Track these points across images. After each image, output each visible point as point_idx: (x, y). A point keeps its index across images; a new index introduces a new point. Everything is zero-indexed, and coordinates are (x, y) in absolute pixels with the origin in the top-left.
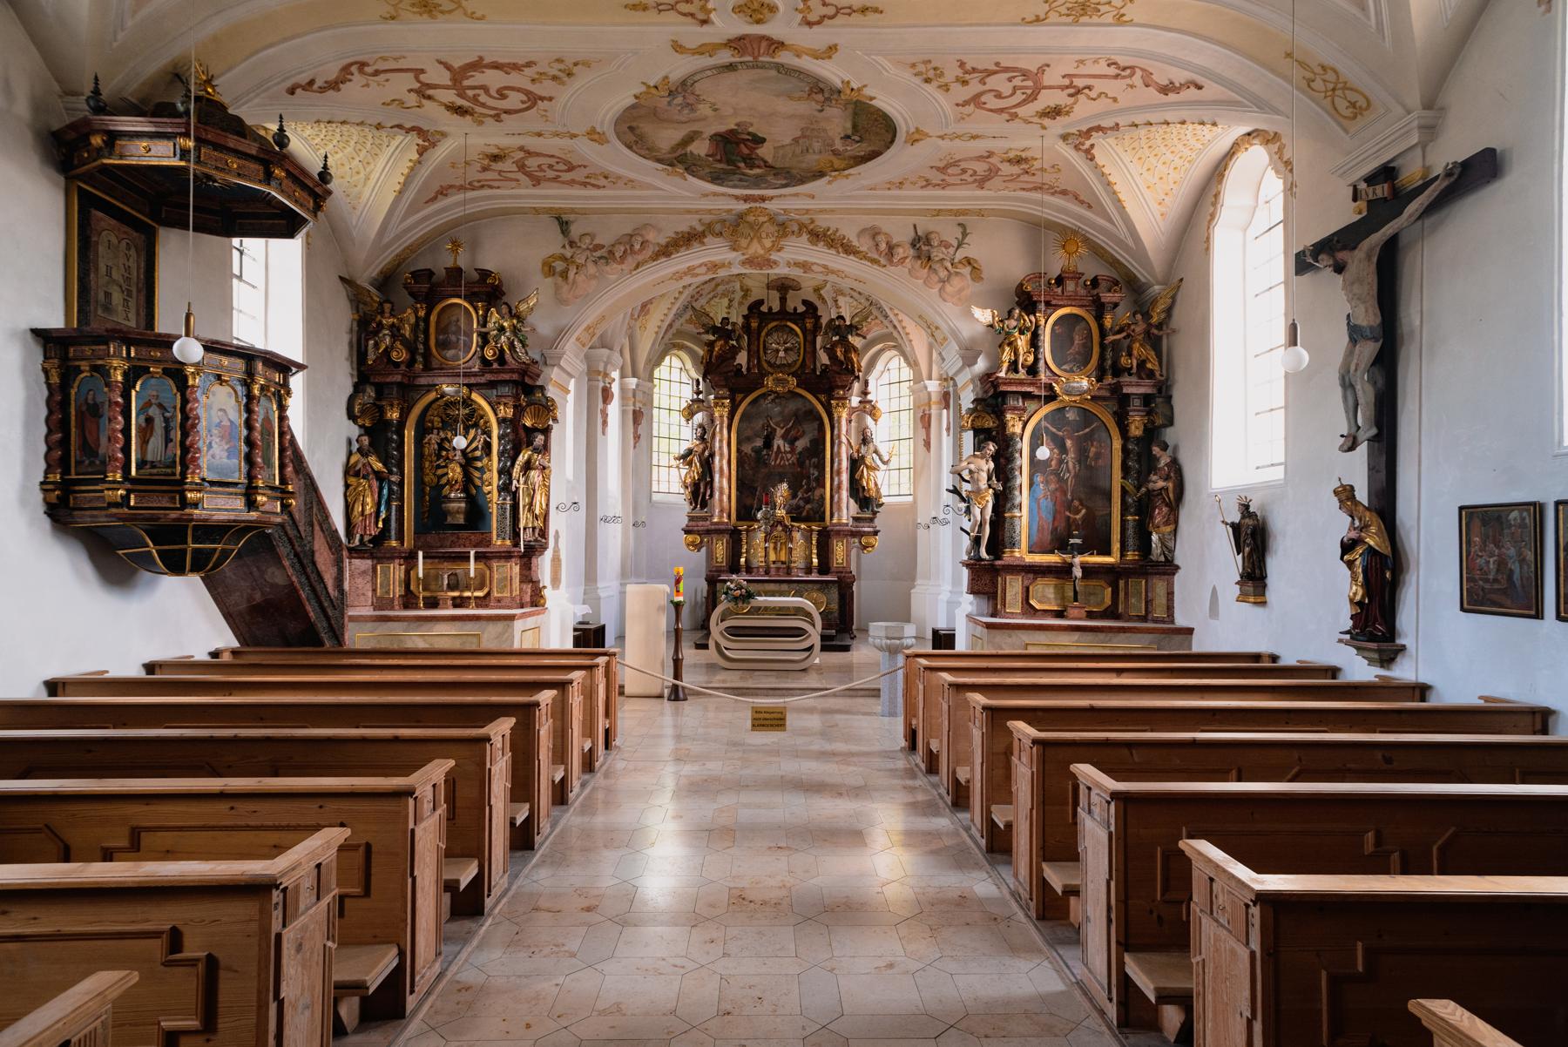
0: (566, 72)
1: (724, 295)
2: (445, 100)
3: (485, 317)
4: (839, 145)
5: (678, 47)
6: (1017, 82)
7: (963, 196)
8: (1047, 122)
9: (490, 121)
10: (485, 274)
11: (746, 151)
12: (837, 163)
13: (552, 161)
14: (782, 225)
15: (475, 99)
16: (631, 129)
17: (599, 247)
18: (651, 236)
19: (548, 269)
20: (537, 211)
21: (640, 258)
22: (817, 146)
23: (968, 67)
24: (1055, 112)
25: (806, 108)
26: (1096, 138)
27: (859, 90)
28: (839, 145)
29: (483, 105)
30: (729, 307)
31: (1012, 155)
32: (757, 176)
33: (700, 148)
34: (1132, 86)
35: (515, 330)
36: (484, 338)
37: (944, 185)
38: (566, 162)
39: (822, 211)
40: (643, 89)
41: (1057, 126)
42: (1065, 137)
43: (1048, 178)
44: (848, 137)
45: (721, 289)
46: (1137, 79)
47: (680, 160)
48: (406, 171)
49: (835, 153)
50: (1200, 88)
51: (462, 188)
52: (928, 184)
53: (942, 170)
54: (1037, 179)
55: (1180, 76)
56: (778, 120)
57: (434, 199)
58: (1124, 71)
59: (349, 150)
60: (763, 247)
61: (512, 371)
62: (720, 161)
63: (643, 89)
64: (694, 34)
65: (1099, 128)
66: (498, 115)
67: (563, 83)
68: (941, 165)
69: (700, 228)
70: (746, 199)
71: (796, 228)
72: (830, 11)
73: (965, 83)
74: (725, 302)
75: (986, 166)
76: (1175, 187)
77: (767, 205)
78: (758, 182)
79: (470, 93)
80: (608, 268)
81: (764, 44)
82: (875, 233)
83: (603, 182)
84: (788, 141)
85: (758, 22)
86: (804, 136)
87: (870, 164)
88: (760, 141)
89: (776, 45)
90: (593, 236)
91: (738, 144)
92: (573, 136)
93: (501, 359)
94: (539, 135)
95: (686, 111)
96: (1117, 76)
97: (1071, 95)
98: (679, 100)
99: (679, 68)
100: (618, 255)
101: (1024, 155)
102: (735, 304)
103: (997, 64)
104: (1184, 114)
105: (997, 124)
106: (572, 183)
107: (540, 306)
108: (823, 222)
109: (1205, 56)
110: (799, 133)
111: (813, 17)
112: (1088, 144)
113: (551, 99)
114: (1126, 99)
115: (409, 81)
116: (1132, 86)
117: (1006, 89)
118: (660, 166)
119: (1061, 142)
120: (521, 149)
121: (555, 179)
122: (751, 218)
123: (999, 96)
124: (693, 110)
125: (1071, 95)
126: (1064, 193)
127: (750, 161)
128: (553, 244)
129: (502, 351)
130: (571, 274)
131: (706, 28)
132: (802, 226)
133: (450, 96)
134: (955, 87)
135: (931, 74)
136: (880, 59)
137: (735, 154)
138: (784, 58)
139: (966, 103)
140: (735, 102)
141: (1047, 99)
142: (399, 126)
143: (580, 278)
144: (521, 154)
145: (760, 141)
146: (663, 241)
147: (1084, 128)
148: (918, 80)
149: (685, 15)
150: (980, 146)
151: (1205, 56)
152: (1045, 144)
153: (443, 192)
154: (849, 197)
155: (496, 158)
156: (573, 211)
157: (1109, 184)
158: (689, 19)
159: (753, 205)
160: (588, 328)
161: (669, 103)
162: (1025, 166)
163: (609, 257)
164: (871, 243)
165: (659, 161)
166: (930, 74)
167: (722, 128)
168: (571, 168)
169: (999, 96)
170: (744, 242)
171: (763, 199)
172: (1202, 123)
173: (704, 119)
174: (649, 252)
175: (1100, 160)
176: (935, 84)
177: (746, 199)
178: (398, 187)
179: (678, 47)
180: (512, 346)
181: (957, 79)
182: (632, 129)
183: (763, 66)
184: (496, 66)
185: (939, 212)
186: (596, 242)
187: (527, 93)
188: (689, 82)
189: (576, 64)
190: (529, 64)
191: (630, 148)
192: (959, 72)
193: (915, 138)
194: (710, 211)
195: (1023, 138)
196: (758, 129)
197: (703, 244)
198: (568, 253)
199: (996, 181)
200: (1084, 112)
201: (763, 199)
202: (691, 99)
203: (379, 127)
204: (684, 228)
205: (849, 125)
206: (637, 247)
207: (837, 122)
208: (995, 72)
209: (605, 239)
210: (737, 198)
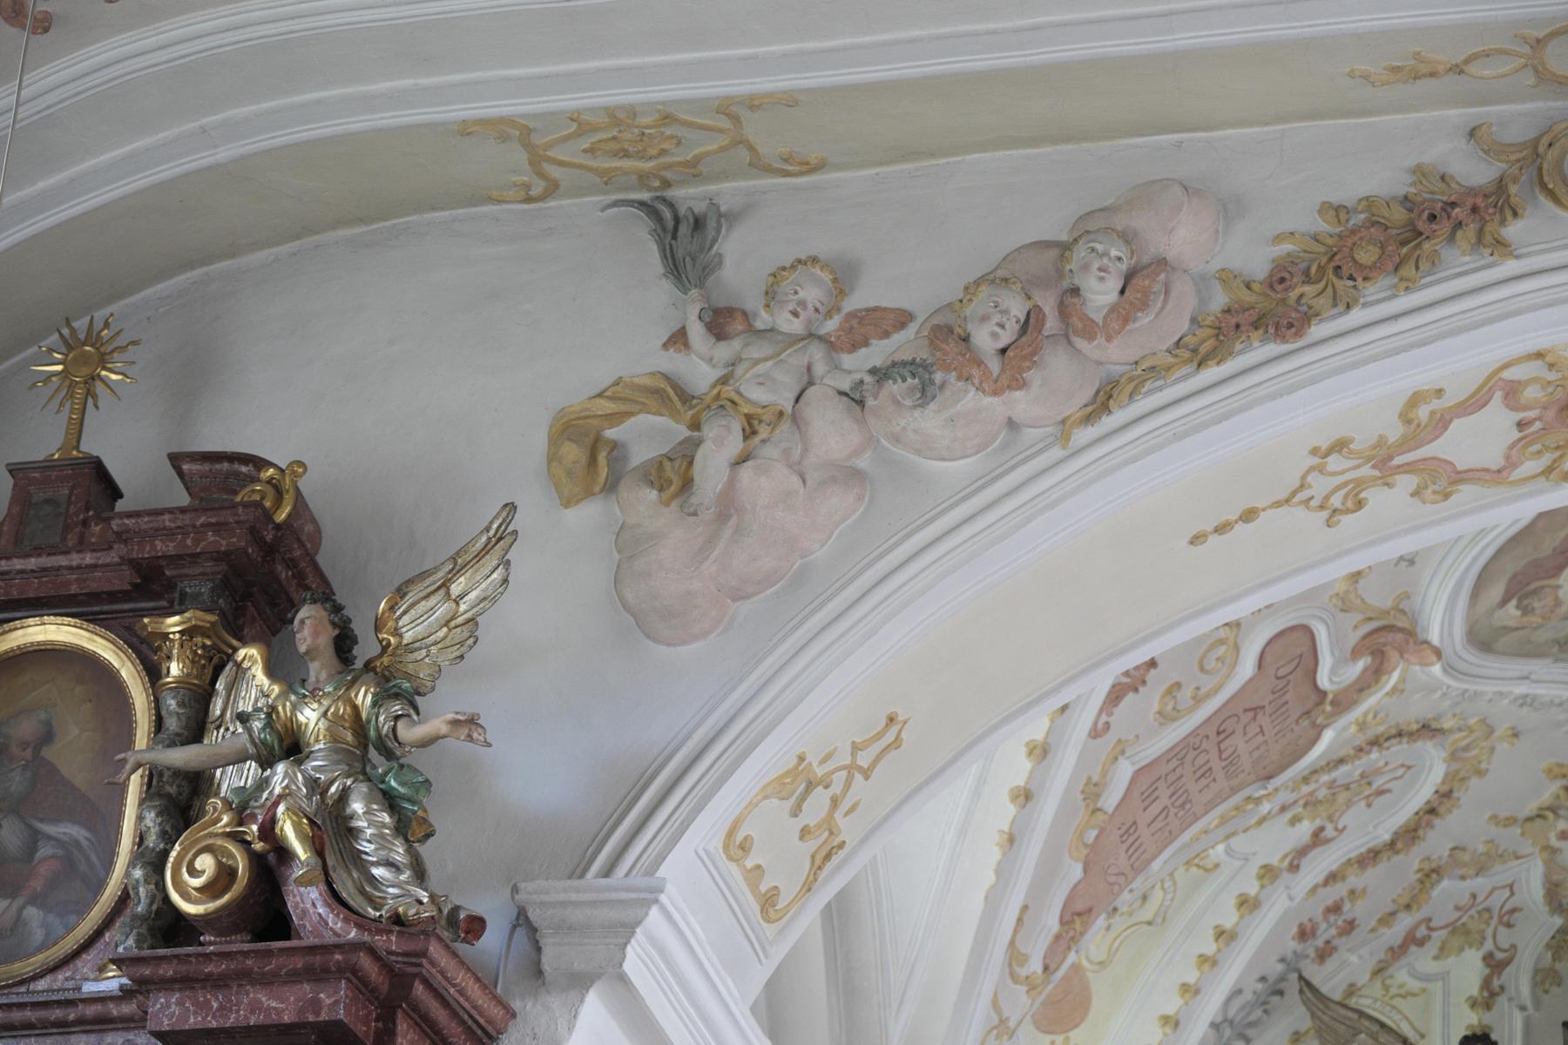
1: (1462, 933)
3: (199, 697)
10: (220, 476)
18: (1184, 238)
19: (588, 455)
21: (1116, 354)
30: (1489, 996)
35: (363, 747)
36: (182, 799)
45: (1449, 893)
61: (322, 964)
69: (1475, 172)
74: (1468, 970)
80: (929, 421)
90: (843, 277)
93: (262, 910)
100: (986, 339)
102: (1520, 979)
107: (526, 680)
128: (612, 325)
129: (270, 864)
130: (713, 462)
143: (763, 484)
146: (1253, 256)
160: (799, 783)
163: (938, 355)
174: (1167, 321)
180: (330, 829)
186: (858, 300)
197: (1502, 247)
198: (699, 368)
204: (1375, 173)
206: (1101, 294)
209: (911, 277)
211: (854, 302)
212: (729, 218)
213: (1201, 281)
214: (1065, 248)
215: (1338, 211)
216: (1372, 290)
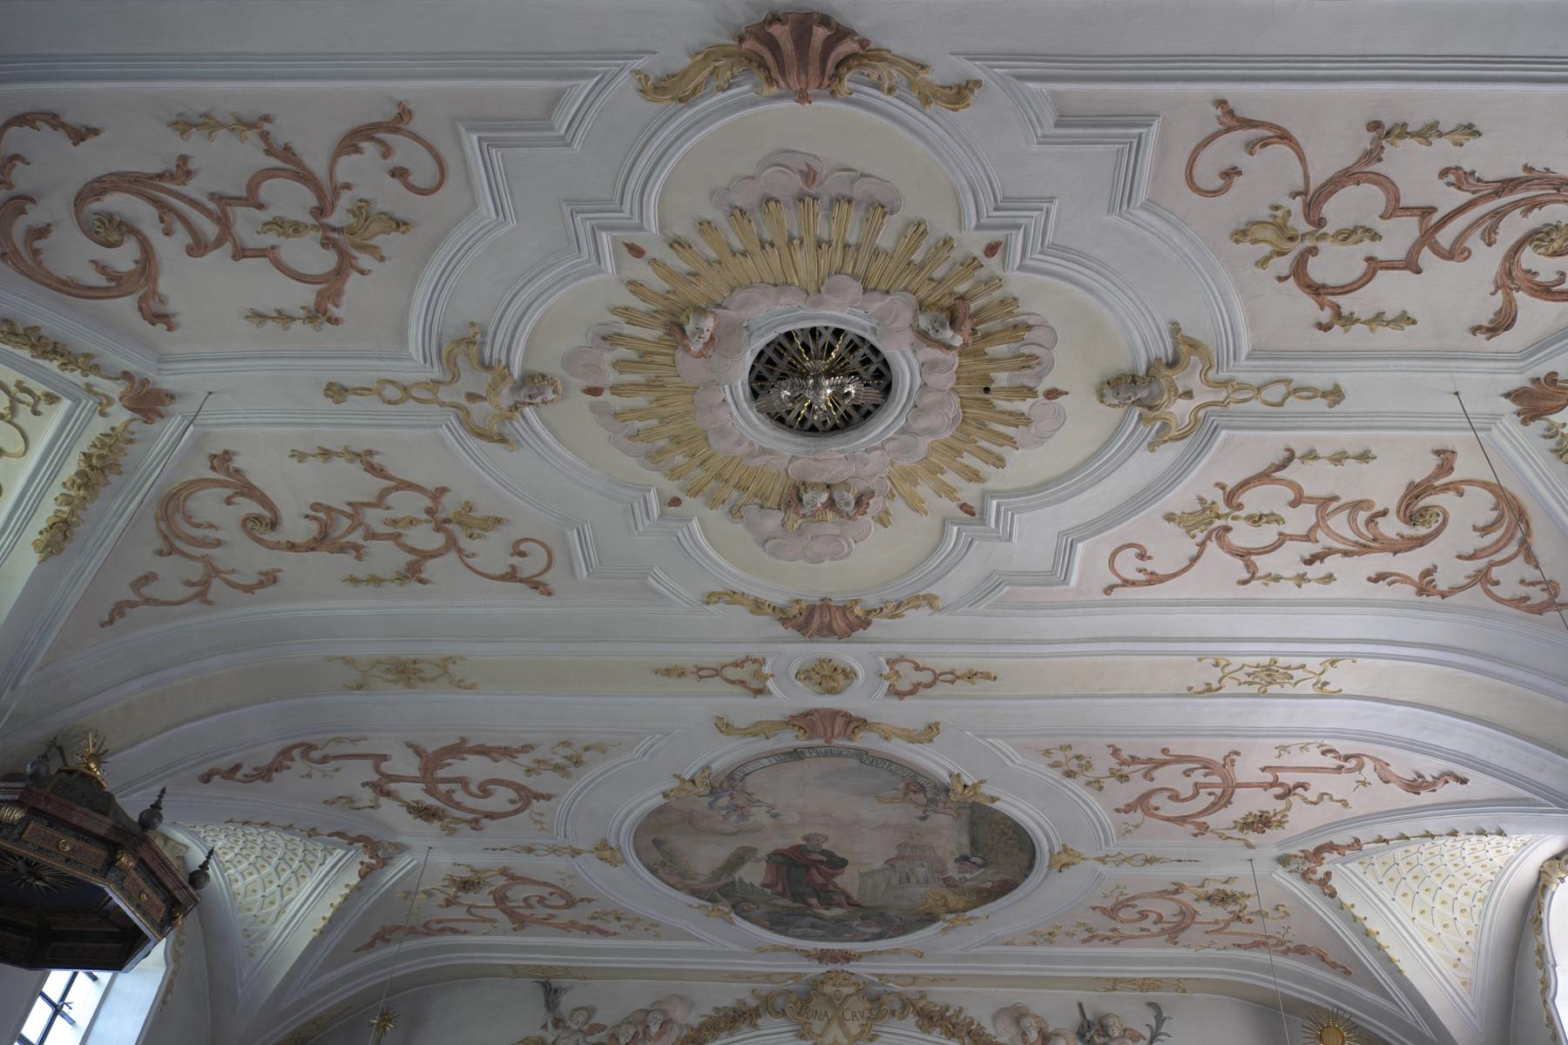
0: (573, 761)
2: (408, 799)
4: (953, 871)
5: (724, 726)
6: (1198, 776)
7: (1148, 957)
8: (1252, 837)
9: (465, 828)
11: (819, 879)
12: (953, 900)
13: (544, 891)
14: (876, 1000)
15: (448, 798)
16: (657, 843)
17: (598, 1028)
18: (679, 1014)
20: (515, 972)
22: (921, 872)
23: (1125, 755)
24: (1261, 822)
25: (901, 814)
26: (1330, 862)
27: (974, 786)
28: (953, 871)
29: (458, 805)
31: (1210, 889)
32: (838, 920)
33: (754, 874)
34: (1364, 783)
37: (1116, 939)
38: (563, 894)
39: (937, 980)
40: (676, 783)
41: (1269, 843)
42: (1284, 861)
43: (1273, 927)
44: (965, 858)
46: (1369, 772)
47: (724, 893)
48: (337, 901)
49: (949, 883)
50: (1464, 781)
51: (413, 932)
52: (1091, 937)
53: (1111, 912)
54: (1257, 928)
55: (1431, 767)
56: (865, 832)
57: (369, 946)
58: (1348, 763)
59: (268, 869)
60: (847, 1034)
62: (782, 894)
63: (676, 783)
64: (745, 709)
65: (1331, 847)
66: (476, 821)
67: (567, 775)
68: (1108, 904)
69: (752, 1003)
70: (822, 957)
71: (897, 1006)
72: (926, 677)
73: (1123, 778)
75: (1175, 908)
76: (1468, 938)
77: (851, 967)
78: (838, 930)
79: (443, 788)
81: (840, 722)
82: (1018, 1015)
83: (613, 926)
84: (879, 864)
85: (831, 691)
86: (901, 857)
87: (1002, 901)
88: (838, 864)
89: (854, 724)
90: (591, 1011)
91: (807, 868)
92: (576, 853)
94: (530, 850)
95: (734, 818)
96: (1339, 769)
97: (1278, 797)
98: (724, 801)
99: (725, 753)
101: (1229, 889)
103: (1165, 751)
104: (1452, 821)
105: (1178, 841)
106: (571, 927)
108: (940, 995)
109: (1461, 737)
110: (894, 853)
111: (903, 686)
112: (1320, 872)
113: (548, 797)
114: (1361, 803)
115: (366, 771)
116: (1364, 783)
117: (1185, 787)
118: (695, 901)
119: (1280, 870)
120: (504, 872)
121: (545, 921)
122: (829, 989)
123: (1175, 797)
124: (743, 816)
125: (1278, 797)
126: (1301, 950)
127: (827, 896)
131: (760, 700)
132: (907, 1004)
133: (414, 793)
134: (1111, 784)
135: (1074, 765)
136: (999, 742)
137: (803, 886)
138: (866, 741)
139: (1129, 808)
140: (800, 806)
141: (1249, 802)
142: (340, 834)
144: (502, 881)
145: (838, 864)
147: (1311, 847)
148: (1056, 774)
149: (733, 682)
150: (1161, 876)
151: (1461, 737)
152: (1257, 872)
153: (383, 937)
154: (976, 957)
155: (466, 885)
156: (568, 972)
157: (1367, 933)
158: (738, 689)
159: (831, 967)
161: (711, 806)
162: (1232, 908)
164: (1013, 1030)
165: (695, 892)
166: (1074, 767)
167: (784, 843)
168: (571, 903)
169: (1175, 797)
170: (817, 1026)
171: (847, 957)
172: (1482, 833)
173: (760, 829)
175: (1345, 895)
176: (1082, 779)
177: (822, 957)
178: (321, 925)
179: (724, 726)
181: (1113, 775)
182: (658, 841)
183: (839, 753)
184: (482, 751)
185: (1114, 984)
187: (518, 788)
188: (739, 775)
189: (587, 749)
190: (526, 749)
191: (654, 872)
192: (1113, 763)
193: (1065, 860)
194: (768, 977)
195: (1222, 863)
196: (834, 844)
197: (756, 1027)
199: (1195, 932)
200: (1302, 819)
201: (847, 957)
202: (741, 800)
203: (312, 833)
204: (728, 1001)
205: (965, 840)
207: (947, 837)
208: (1164, 763)
210: (808, 955)
211: (593, 1021)
212: (566, 990)
213: (681, 1026)
214: (648, 1012)
215: (717, 1010)
216: (722, 1035)
